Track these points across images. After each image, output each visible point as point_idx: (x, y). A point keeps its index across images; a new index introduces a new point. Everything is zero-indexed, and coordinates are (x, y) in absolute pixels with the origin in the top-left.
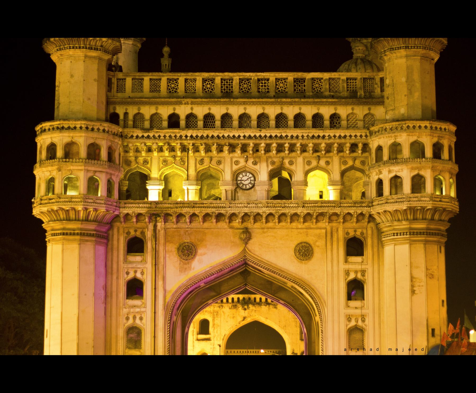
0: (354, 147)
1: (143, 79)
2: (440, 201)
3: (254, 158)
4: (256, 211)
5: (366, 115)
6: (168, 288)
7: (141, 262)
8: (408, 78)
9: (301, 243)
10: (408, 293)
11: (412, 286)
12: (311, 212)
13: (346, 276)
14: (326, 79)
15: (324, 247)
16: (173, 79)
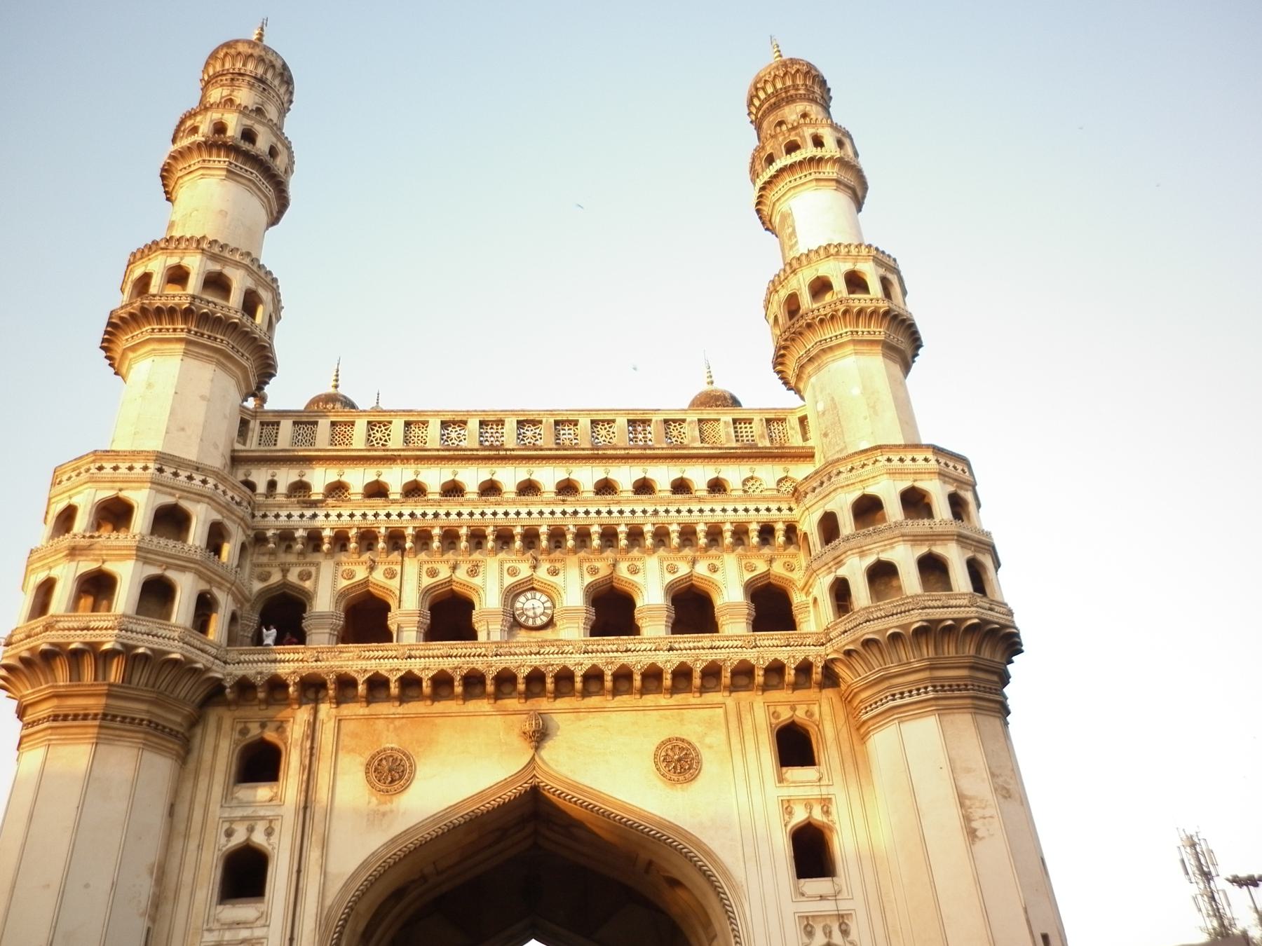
0: (767, 532)
1: (316, 423)
2: (991, 609)
3: (551, 561)
4: (558, 661)
5: (780, 481)
6: (333, 868)
7: (271, 800)
8: (864, 388)
9: (669, 740)
10: (959, 838)
11: (967, 819)
12: (689, 661)
13: (787, 817)
14: (691, 422)
15: (725, 748)
16: (380, 422)
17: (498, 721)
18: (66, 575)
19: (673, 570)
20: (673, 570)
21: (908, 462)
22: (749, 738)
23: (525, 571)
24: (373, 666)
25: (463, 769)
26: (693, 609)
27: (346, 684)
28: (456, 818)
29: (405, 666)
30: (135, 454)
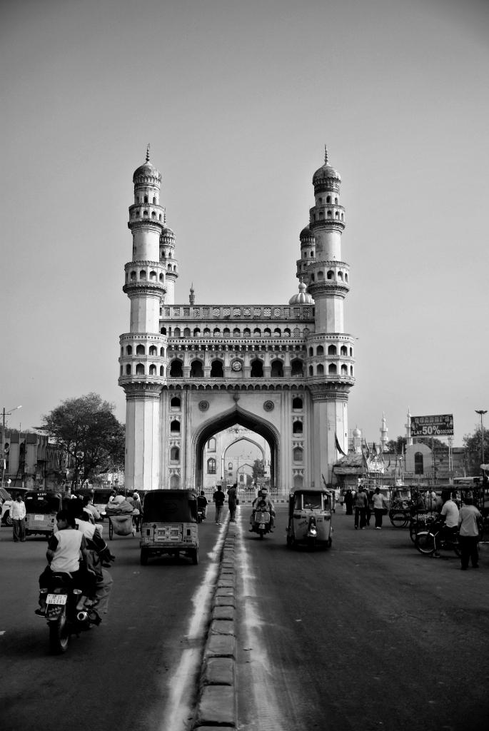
0: (298, 347)
4: (243, 383)
17: (228, 395)
18: (134, 365)
19: (272, 357)
20: (272, 357)
21: (332, 338)
22: (286, 399)
23: (235, 357)
24: (200, 383)
25: (220, 407)
26: (277, 365)
27: (193, 386)
28: (219, 416)
29: (207, 383)
30: (143, 334)
